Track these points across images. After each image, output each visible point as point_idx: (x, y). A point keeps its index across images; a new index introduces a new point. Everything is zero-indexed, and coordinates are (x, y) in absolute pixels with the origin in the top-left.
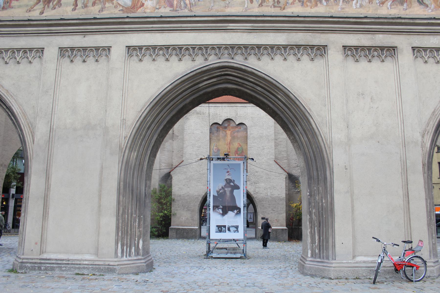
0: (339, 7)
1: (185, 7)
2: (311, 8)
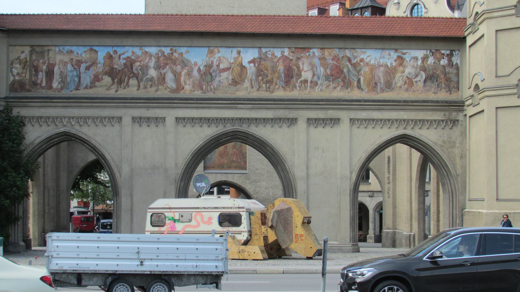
0: (307, 91)
1: (211, 91)
2: (289, 92)
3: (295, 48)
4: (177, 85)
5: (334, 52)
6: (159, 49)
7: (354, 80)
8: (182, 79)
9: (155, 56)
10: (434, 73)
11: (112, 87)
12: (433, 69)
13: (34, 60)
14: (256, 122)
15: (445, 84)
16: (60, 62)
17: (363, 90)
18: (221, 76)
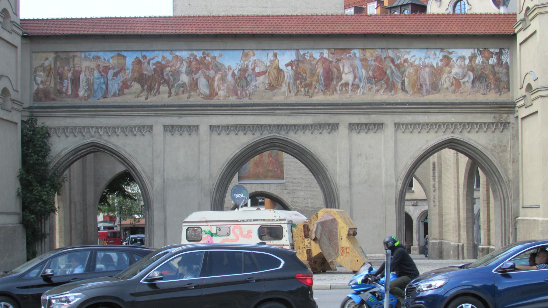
0: (349, 94)
1: (246, 96)
2: (330, 96)
3: (335, 49)
4: (210, 91)
5: (377, 53)
6: (190, 53)
7: (398, 82)
8: (216, 84)
9: (187, 60)
10: (483, 73)
11: (141, 95)
12: (481, 69)
13: (59, 67)
14: (295, 129)
15: (495, 85)
16: (86, 69)
17: (407, 92)
18: (256, 81)
